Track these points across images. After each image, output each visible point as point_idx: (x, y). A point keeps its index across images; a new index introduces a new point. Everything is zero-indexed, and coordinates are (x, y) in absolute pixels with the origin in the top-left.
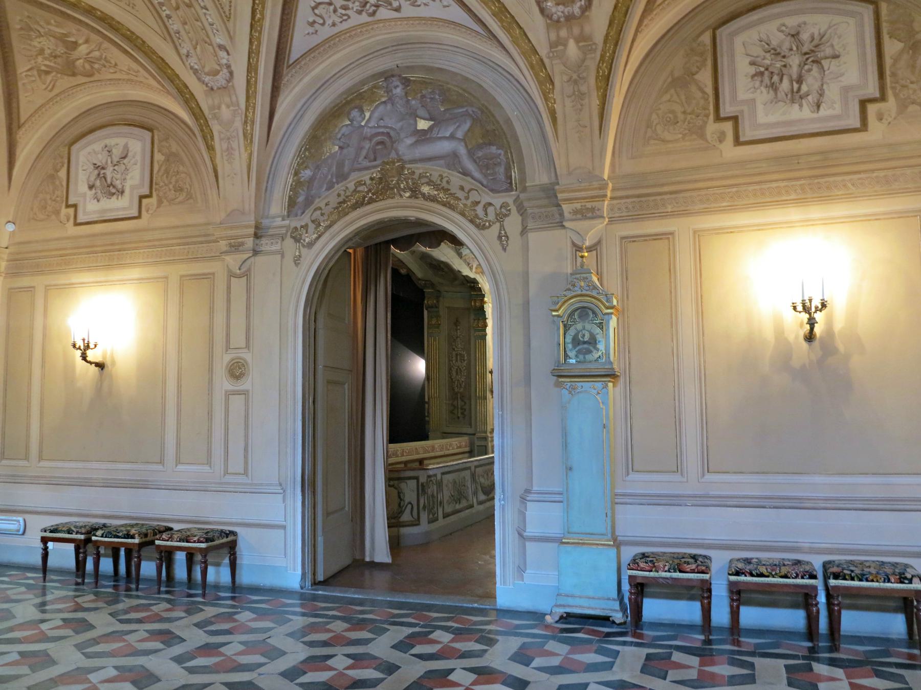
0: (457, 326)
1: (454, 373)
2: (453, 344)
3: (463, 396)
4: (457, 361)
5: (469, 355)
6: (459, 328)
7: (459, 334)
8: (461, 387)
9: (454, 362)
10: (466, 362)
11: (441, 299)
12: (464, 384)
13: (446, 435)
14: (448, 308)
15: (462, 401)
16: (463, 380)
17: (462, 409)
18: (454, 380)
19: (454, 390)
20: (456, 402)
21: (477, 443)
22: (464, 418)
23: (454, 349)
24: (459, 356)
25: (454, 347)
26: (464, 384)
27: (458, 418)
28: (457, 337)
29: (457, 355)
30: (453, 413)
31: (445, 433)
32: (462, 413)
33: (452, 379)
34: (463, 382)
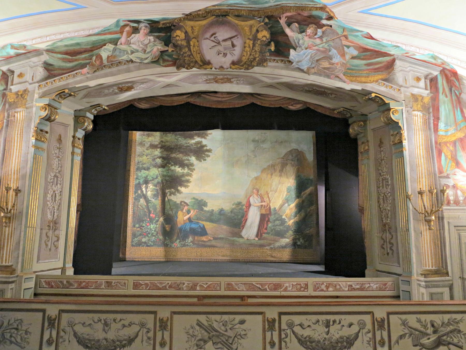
0: (380, 148)
1: (381, 201)
2: (380, 168)
3: (390, 228)
4: (383, 187)
5: (392, 179)
6: (382, 149)
7: (383, 156)
8: (387, 217)
9: (381, 188)
10: (390, 186)
11: (368, 122)
12: (390, 213)
13: (379, 273)
14: (372, 130)
15: (390, 233)
16: (389, 208)
17: (390, 243)
18: (382, 209)
19: (382, 221)
20: (385, 234)
21: (403, 287)
22: (392, 254)
23: (380, 174)
24: (384, 181)
25: (380, 172)
26: (390, 213)
27: (388, 254)
28: (382, 160)
29: (383, 180)
30: (384, 248)
31: (378, 271)
32: (391, 249)
33: (380, 208)
34: (389, 211)
